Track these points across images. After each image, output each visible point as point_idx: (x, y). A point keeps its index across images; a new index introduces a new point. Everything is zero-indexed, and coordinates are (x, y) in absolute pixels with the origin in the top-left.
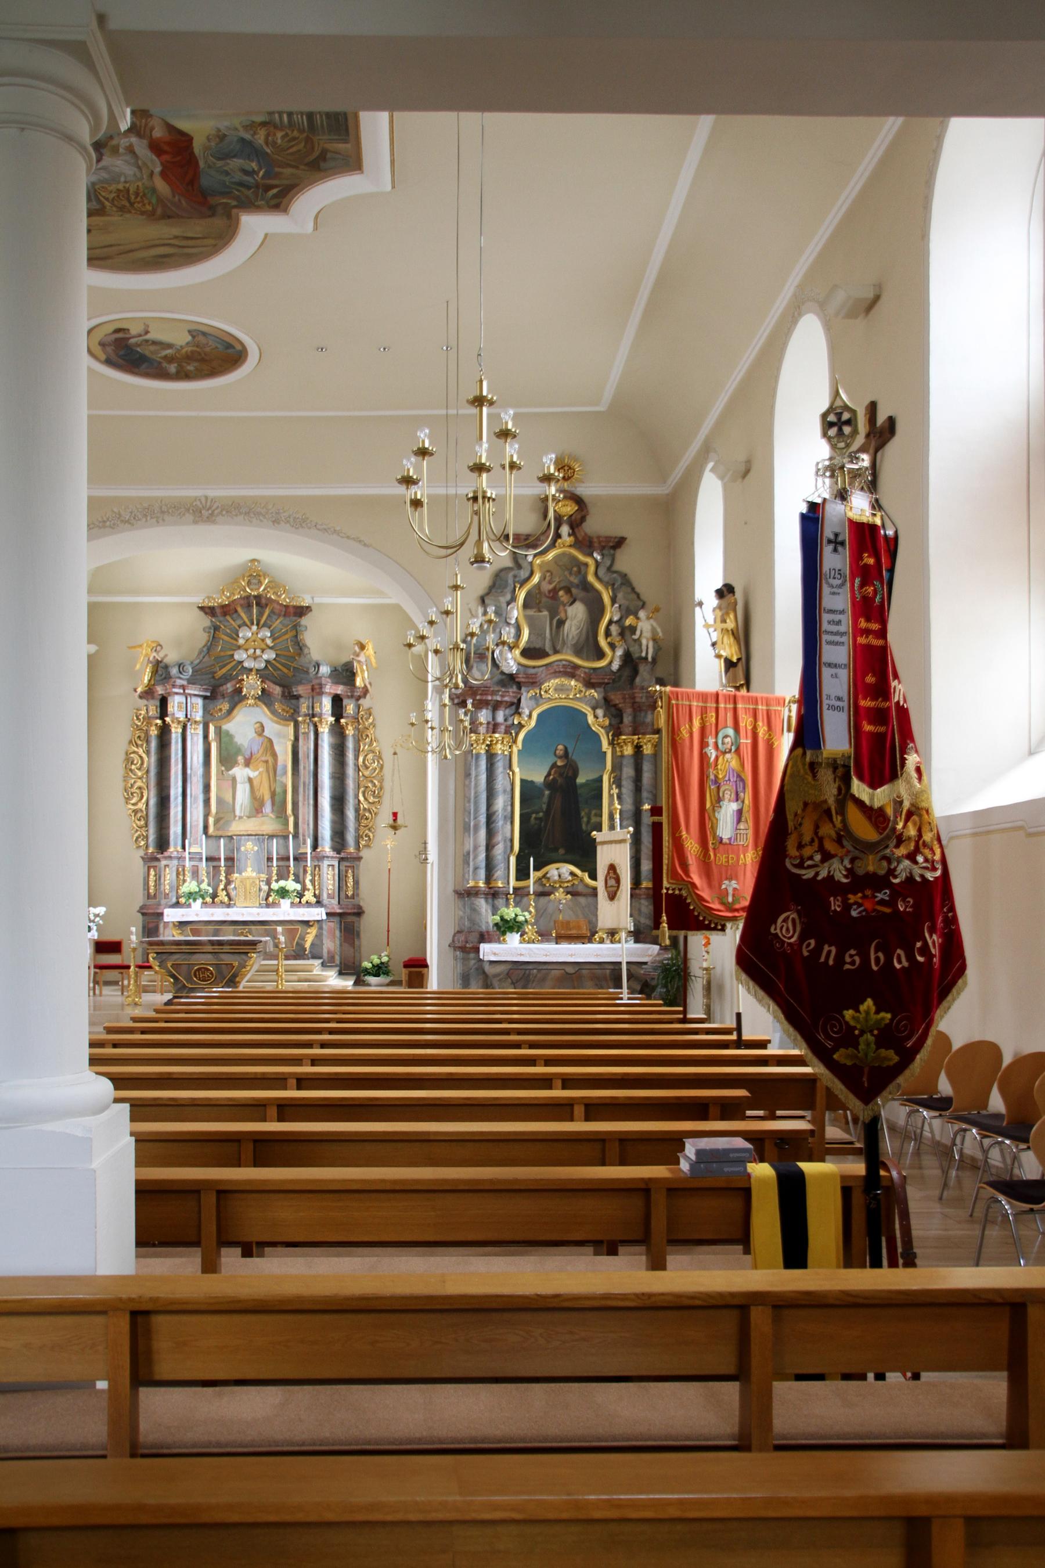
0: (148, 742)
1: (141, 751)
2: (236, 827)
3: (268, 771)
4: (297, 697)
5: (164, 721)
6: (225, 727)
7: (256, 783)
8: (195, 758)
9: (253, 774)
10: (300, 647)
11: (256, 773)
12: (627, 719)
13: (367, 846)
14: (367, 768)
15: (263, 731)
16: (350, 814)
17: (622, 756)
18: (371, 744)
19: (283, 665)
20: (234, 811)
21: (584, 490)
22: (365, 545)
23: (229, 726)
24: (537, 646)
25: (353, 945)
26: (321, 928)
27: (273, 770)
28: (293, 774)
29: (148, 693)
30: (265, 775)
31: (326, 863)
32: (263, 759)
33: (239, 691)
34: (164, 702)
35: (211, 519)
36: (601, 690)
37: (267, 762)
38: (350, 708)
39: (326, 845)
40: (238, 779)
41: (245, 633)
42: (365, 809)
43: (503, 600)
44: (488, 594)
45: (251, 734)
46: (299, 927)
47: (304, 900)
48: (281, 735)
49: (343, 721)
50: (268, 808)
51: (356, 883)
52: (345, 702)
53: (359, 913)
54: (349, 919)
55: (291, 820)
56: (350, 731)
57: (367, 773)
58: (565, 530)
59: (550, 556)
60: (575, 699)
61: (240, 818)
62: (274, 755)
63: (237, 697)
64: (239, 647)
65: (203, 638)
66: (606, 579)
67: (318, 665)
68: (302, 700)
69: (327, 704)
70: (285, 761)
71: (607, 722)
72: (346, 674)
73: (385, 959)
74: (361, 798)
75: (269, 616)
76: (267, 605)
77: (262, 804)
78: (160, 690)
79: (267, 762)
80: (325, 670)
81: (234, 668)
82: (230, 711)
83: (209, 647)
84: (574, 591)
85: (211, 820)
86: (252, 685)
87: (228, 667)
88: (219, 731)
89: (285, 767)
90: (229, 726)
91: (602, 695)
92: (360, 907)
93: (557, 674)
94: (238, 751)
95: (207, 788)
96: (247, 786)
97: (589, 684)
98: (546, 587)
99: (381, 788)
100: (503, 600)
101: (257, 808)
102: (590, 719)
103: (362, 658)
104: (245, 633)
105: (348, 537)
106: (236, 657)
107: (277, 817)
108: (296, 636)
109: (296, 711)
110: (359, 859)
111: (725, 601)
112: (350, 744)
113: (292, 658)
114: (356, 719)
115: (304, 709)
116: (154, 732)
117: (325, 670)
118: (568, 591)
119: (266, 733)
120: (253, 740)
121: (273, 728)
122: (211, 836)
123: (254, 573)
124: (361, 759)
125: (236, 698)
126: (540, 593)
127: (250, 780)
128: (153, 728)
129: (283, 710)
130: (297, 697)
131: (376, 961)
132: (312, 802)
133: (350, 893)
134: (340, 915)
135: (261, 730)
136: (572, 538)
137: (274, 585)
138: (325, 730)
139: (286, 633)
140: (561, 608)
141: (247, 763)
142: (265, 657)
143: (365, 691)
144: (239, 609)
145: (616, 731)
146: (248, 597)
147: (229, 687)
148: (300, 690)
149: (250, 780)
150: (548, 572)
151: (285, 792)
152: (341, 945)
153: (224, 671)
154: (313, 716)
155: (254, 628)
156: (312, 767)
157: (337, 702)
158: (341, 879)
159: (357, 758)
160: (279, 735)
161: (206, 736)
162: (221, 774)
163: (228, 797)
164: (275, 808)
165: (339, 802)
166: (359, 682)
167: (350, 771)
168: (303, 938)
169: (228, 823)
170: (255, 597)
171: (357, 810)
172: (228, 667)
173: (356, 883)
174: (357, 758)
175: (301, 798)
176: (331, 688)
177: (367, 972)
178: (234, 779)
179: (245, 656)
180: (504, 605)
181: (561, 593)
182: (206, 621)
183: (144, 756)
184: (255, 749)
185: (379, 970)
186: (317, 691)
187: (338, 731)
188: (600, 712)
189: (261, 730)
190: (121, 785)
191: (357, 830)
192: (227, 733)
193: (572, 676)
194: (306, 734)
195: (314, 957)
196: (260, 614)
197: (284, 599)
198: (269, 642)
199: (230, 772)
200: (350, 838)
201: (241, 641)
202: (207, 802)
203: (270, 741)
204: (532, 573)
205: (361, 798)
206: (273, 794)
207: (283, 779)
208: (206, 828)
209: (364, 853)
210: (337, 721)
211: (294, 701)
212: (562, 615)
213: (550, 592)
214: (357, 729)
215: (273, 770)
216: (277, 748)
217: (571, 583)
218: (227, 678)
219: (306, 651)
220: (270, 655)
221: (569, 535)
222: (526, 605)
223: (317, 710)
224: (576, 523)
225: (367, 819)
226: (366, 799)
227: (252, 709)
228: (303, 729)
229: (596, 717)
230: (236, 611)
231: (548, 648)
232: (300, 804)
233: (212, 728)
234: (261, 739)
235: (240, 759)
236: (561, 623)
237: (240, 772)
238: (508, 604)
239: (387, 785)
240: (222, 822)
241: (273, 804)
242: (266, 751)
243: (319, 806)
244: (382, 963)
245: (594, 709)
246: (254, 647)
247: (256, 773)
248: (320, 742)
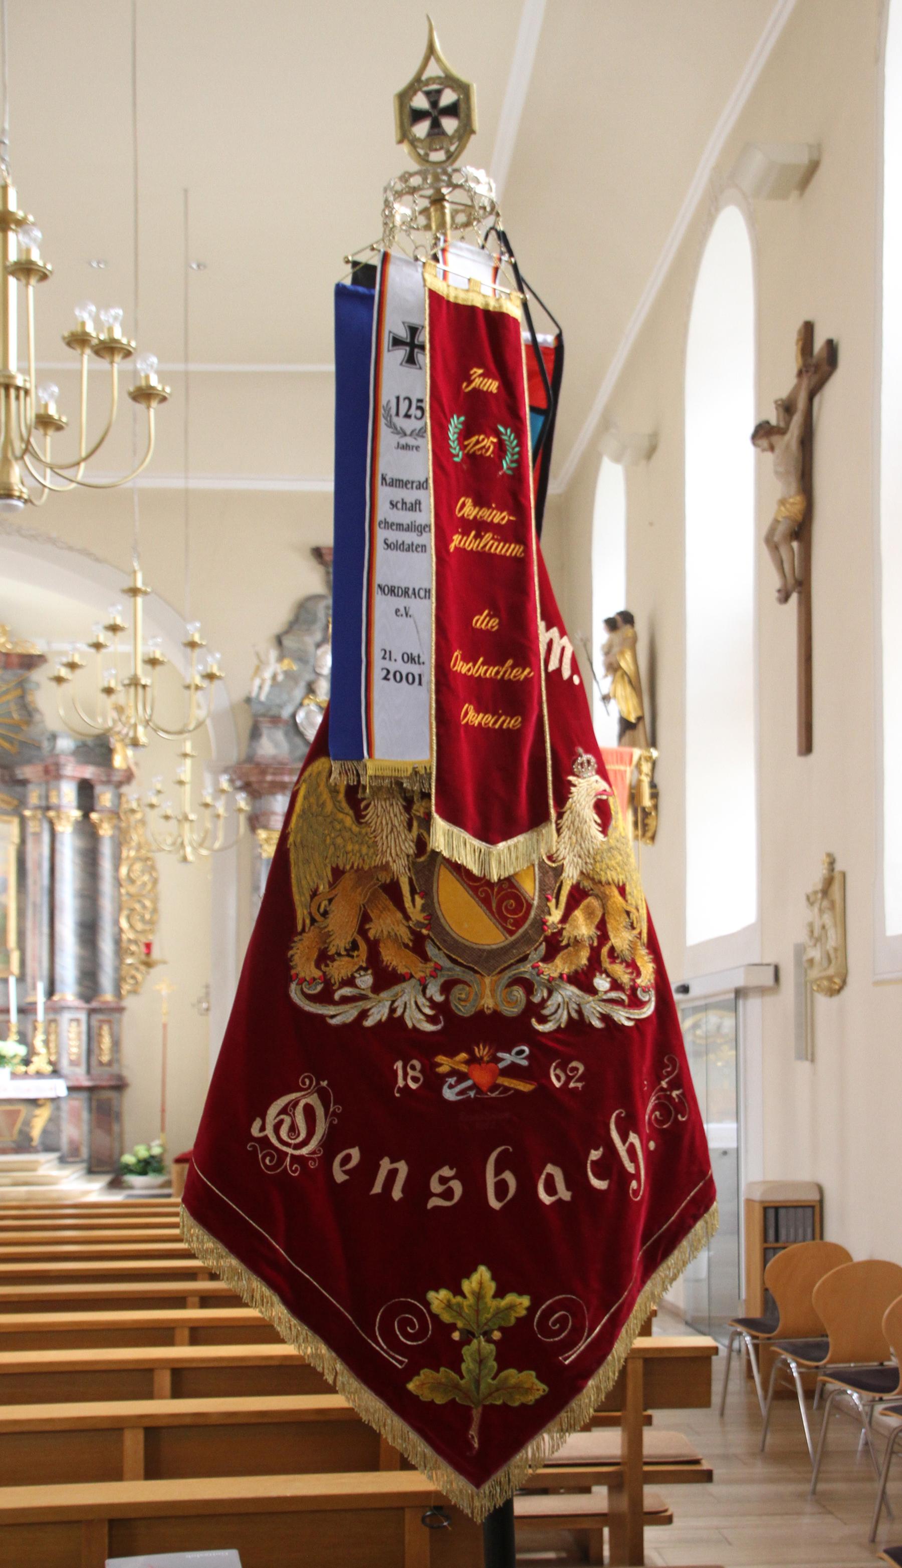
4: (24, 783)
10: (28, 712)
13: (134, 992)
14: (132, 881)
16: (106, 947)
25: (109, 1131)
26: (58, 1108)
31: (66, 1016)
38: (105, 798)
39: (69, 991)
42: (130, 941)
46: (24, 1109)
47: (32, 1069)
49: (94, 816)
51: (116, 1044)
52: (98, 789)
54: (104, 1096)
55: (15, 957)
56: (106, 831)
57: (133, 890)
67: (54, 737)
68: (31, 787)
69: (68, 793)
72: (98, 750)
73: (156, 1151)
74: (124, 924)
92: (120, 1078)
99: (155, 911)
108: (22, 697)
109: (22, 803)
112: (106, 850)
113: (16, 727)
114: (115, 814)
115: (34, 796)
117: (65, 744)
131: (143, 1152)
132: (45, 930)
133: (105, 1058)
134: (91, 1089)
138: (66, 831)
139: (6, 692)
143: (129, 777)
148: (27, 772)
152: (91, 1132)
154: (48, 808)
157: (86, 790)
158: (92, 1038)
159: (116, 867)
165: (89, 930)
166: (118, 761)
167: (107, 886)
168: (27, 1123)
171: (118, 941)
173: (116, 1044)
174: (116, 867)
175: (29, 924)
176: (74, 770)
177: (128, 1169)
185: (147, 1166)
186: (53, 773)
187: (88, 830)
191: (117, 969)
194: (38, 836)
195: (48, 1148)
200: (106, 980)
205: (124, 924)
209: (129, 1002)
210: (86, 816)
211: (19, 789)
214: (117, 828)
219: (37, 717)
226: (132, 927)
228: (32, 827)
239: (163, 906)
244: (152, 1157)
248: (58, 846)
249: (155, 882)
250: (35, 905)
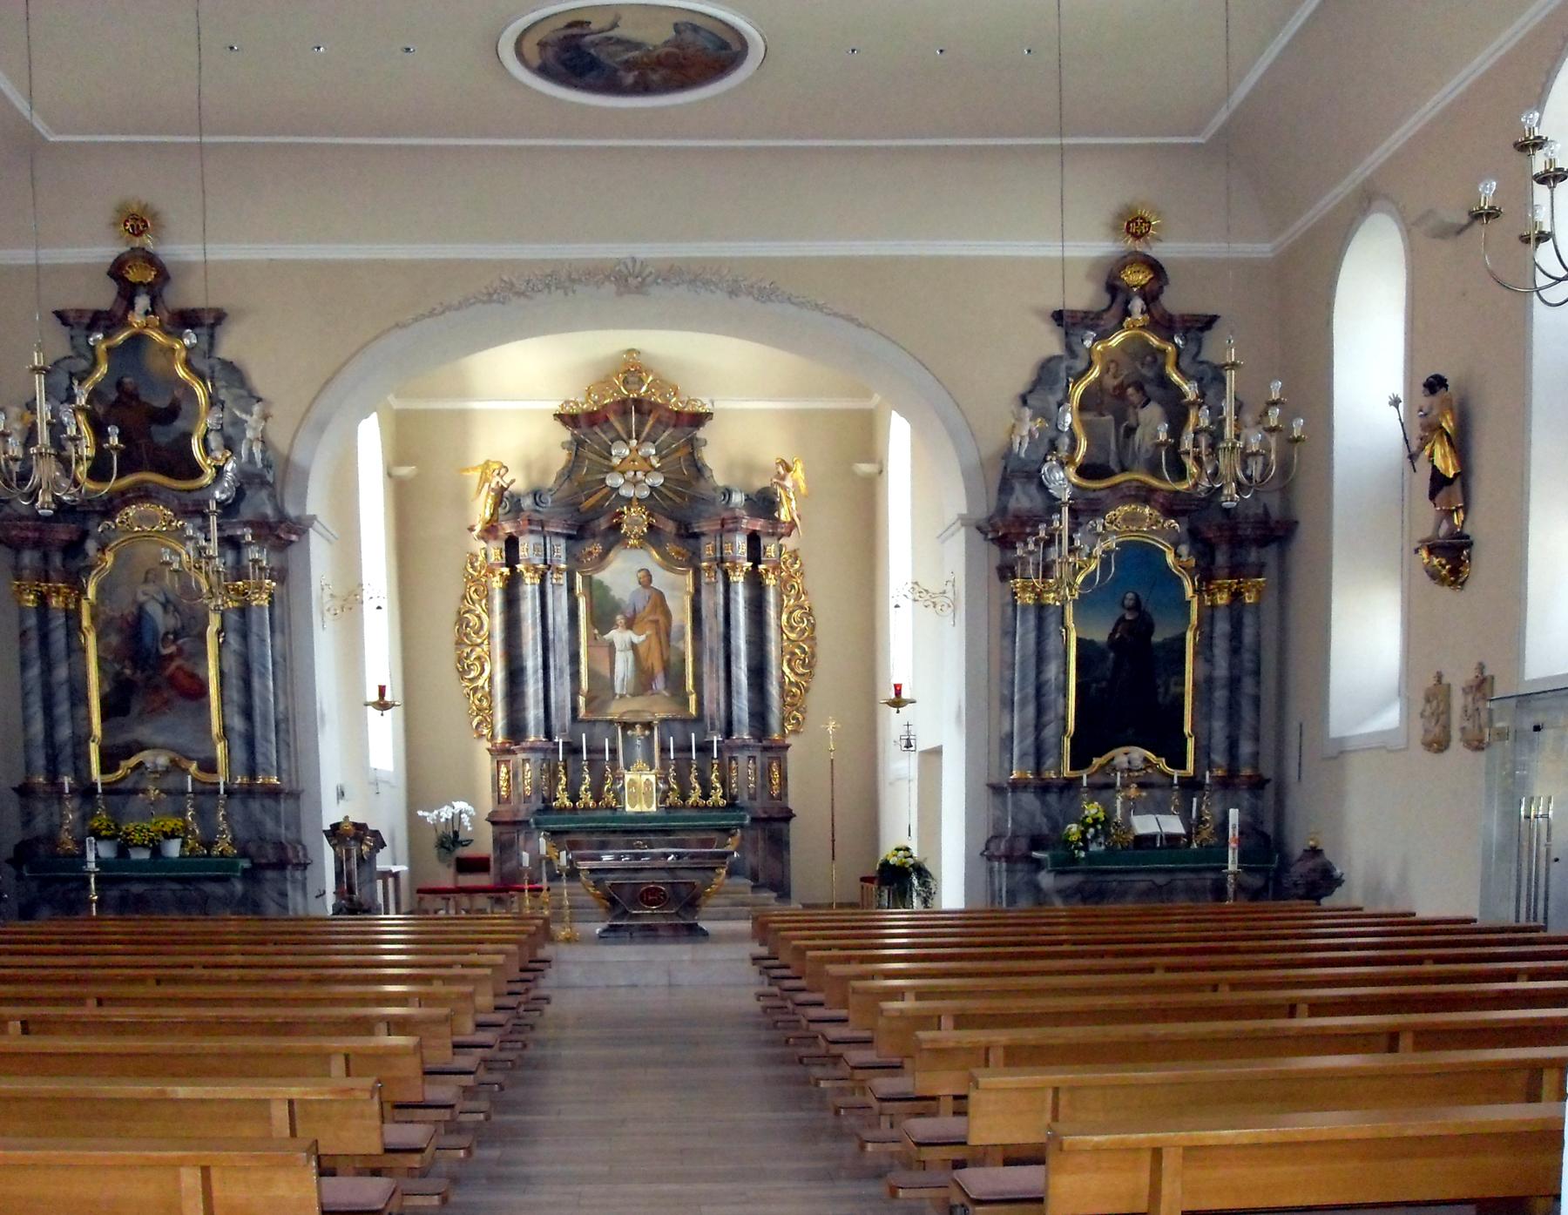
0: (489, 598)
1: (479, 610)
2: (616, 710)
3: (657, 633)
4: (696, 536)
5: (513, 570)
6: (597, 576)
7: (642, 650)
8: (558, 618)
9: (637, 639)
10: (698, 469)
11: (643, 637)
12: (1221, 558)
16: (774, 690)
17: (1214, 607)
18: (798, 597)
19: (675, 492)
20: (613, 687)
21: (1158, 251)
22: (859, 325)
24: (1099, 462)
29: (490, 530)
33: (618, 526)
34: (512, 544)
35: (641, 289)
36: (1185, 519)
37: (656, 622)
38: (770, 548)
39: (743, 734)
41: (620, 451)
43: (1053, 399)
44: (1030, 392)
45: (634, 585)
47: (710, 802)
48: (676, 588)
49: (761, 567)
50: (659, 684)
52: (764, 541)
53: (788, 816)
55: (693, 699)
56: (771, 581)
57: (793, 636)
58: (1137, 305)
59: (1116, 340)
60: (1151, 532)
61: (622, 696)
63: (614, 536)
64: (612, 469)
65: (561, 458)
66: (1191, 371)
67: (728, 492)
68: (704, 540)
69: (741, 543)
70: (683, 621)
71: (1193, 562)
72: (765, 503)
75: (653, 426)
76: (650, 412)
78: (508, 528)
80: (738, 498)
81: (606, 497)
82: (604, 556)
83: (569, 472)
84: (1147, 387)
85: (582, 700)
86: (635, 519)
87: (599, 495)
88: (588, 582)
89: (683, 628)
91: (1186, 527)
93: (1126, 499)
94: (616, 607)
95: (575, 658)
96: (630, 654)
97: (1169, 512)
98: (1111, 382)
100: (1053, 399)
101: (643, 681)
102: (1170, 559)
103: (788, 483)
104: (620, 451)
105: (835, 315)
106: (608, 482)
107: (673, 695)
108: (692, 454)
110: (787, 747)
111: (1436, 399)
112: (771, 597)
113: (686, 484)
115: (708, 549)
116: (497, 584)
117: (738, 498)
118: (1140, 387)
120: (635, 593)
121: (663, 579)
122: (582, 721)
123: (632, 368)
124: (784, 617)
125: (612, 538)
126: (1102, 390)
127: (634, 647)
128: (498, 578)
129: (678, 553)
130: (696, 536)
132: (722, 674)
133: (775, 793)
135: (646, 579)
136: (1147, 317)
137: (661, 384)
138: (738, 579)
140: (1131, 410)
141: (630, 625)
142: (649, 481)
143: (793, 525)
144: (612, 418)
145: (1205, 575)
146: (624, 401)
147: (603, 524)
149: (634, 647)
150: (1111, 361)
153: (592, 501)
155: (634, 442)
156: (722, 629)
157: (754, 539)
159: (779, 617)
160: (674, 587)
161: (571, 588)
162: (592, 639)
166: (784, 515)
167: (772, 633)
169: (605, 704)
170: (635, 400)
172: (599, 495)
173: (784, 778)
174: (779, 617)
175: (706, 669)
176: (747, 523)
178: (612, 646)
179: (621, 481)
180: (1054, 407)
181: (1130, 390)
182: (565, 434)
183: (484, 616)
184: (639, 606)
186: (727, 526)
188: (1184, 549)
189: (646, 579)
190: (453, 656)
191: (782, 711)
192: (601, 583)
193: (1146, 502)
194: (713, 585)
196: (641, 424)
197: (675, 404)
198: (655, 462)
200: (774, 720)
201: (616, 461)
202: (575, 675)
203: (661, 595)
204: (1091, 364)
206: (666, 668)
207: (680, 645)
208: (575, 709)
210: (755, 567)
211: (691, 541)
212: (1132, 421)
213: (1115, 388)
215: (664, 632)
216: (669, 603)
217: (1143, 377)
218: (597, 511)
219: (707, 474)
220: (657, 480)
221: (1143, 313)
222: (1083, 407)
223: (728, 552)
224: (1151, 296)
225: (794, 695)
227: (634, 552)
229: (1177, 555)
230: (607, 420)
231: (1113, 464)
232: (705, 677)
233: (579, 578)
234: (647, 592)
235: (619, 619)
236: (1130, 431)
237: (620, 636)
238: (1060, 405)
240: (596, 703)
241: (666, 676)
242: (654, 607)
243: (734, 679)
245: (1176, 545)
246: (634, 470)
247: (643, 637)
248: (732, 595)
249: (813, 627)
250: (711, 651)
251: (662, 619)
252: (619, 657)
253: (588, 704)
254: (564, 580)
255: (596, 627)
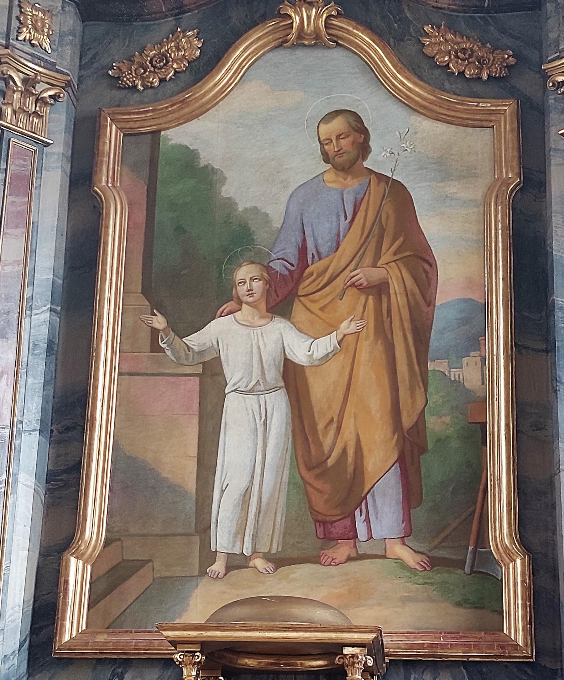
7: (319, 390)
9: (301, 349)
11: (326, 344)
15: (364, 149)
20: (203, 528)
23: (199, 135)
27: (409, 328)
28: (518, 348)
30: (368, 352)
32: (365, 274)
37: (380, 290)
40: (234, 373)
45: (304, 164)
50: (383, 516)
61: (236, 563)
62: (420, 260)
77: (351, 493)
79: (380, 290)
85: (77, 574)
90: (199, 135)
94: (240, 239)
96: (278, 405)
107: (434, 563)
119: (378, 160)
120: (313, 186)
121: (406, 138)
122: (67, 662)
127: (292, 377)
129: (466, 55)
135: (349, 145)
141: (281, 300)
149: (292, 377)
151: (477, 434)
160: (443, 167)
163: (177, 461)
164: (420, 514)
169: (170, 588)
178: (211, 373)
184: (321, 232)
189: (349, 145)
192: (188, 161)
199: (194, 340)
203: (398, 195)
206: (411, 447)
207: (469, 373)
216: (432, 226)
233: (112, 135)
234: (353, 185)
235: (246, 275)
237: (243, 340)
240: (133, 587)
241: (411, 496)
242: (375, 238)
247: (326, 344)
251: (398, 280)
252: (237, 412)
253: (102, 590)
254: (56, 128)
255: (157, 306)
